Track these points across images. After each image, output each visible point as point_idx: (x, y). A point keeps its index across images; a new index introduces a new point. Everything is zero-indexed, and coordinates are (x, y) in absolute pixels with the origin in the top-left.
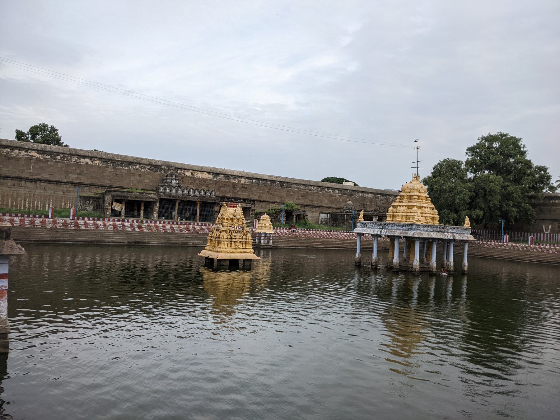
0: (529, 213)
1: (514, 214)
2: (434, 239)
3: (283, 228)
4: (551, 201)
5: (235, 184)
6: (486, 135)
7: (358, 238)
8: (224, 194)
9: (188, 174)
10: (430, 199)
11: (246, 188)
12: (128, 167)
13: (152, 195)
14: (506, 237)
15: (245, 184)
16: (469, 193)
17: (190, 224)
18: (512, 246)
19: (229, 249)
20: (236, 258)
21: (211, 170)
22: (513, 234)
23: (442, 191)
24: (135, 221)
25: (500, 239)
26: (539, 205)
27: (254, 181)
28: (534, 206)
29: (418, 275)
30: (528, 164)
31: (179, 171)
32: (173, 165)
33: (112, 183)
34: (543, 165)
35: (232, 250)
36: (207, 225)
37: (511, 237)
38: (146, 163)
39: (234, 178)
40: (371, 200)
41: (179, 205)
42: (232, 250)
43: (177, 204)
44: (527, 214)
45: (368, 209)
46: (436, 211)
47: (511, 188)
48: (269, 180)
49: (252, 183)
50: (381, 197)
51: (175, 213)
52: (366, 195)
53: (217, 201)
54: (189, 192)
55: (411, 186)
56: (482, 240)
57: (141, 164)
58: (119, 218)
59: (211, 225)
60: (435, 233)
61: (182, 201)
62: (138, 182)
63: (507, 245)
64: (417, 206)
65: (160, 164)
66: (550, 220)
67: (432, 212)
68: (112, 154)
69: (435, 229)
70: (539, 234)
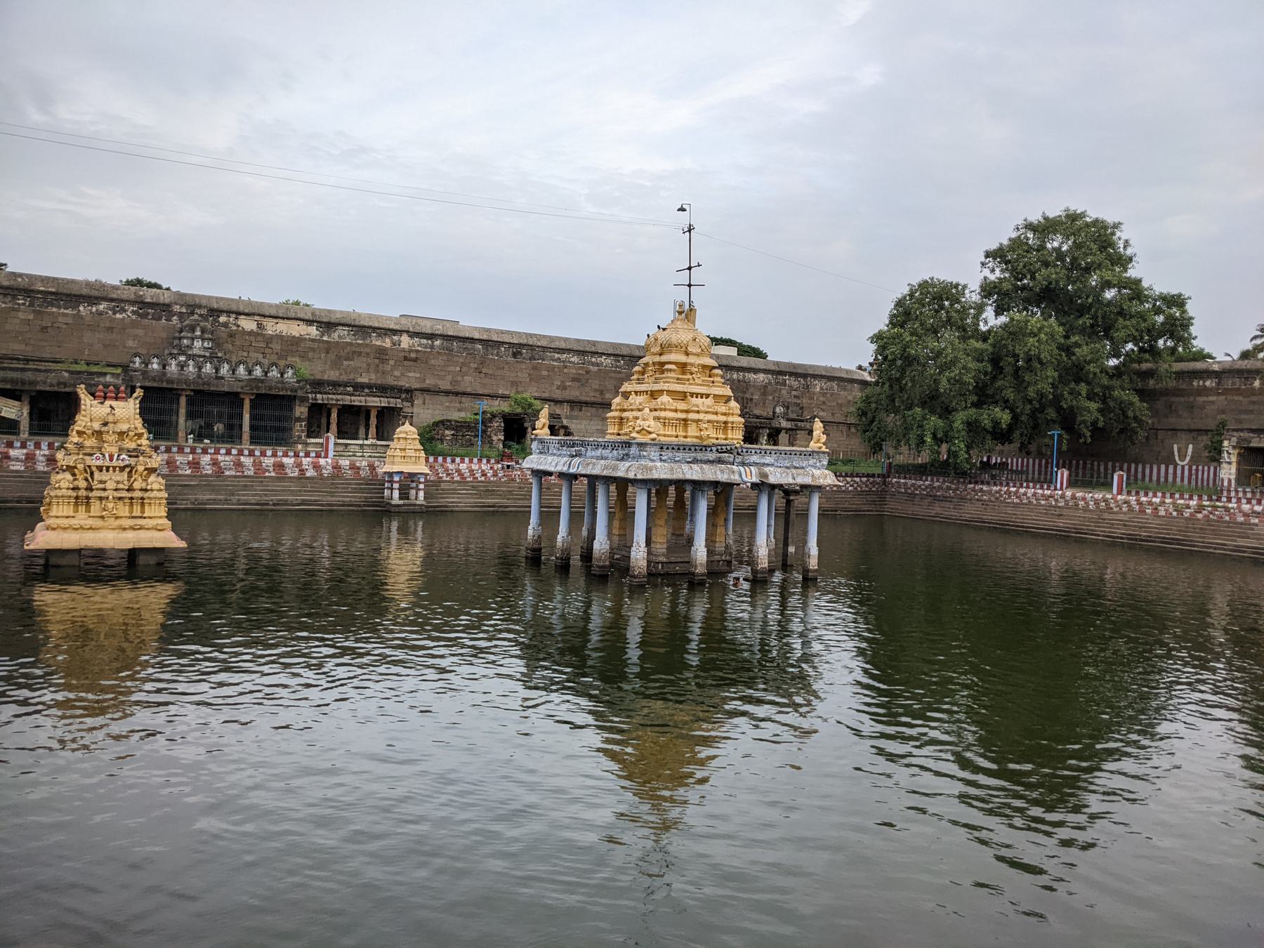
0: (1130, 414)
1: (1088, 418)
2: (698, 485)
3: (480, 461)
4: (1195, 383)
5: (382, 352)
6: (1035, 218)
7: (533, 481)
8: (352, 376)
9: (248, 324)
10: (718, 371)
11: (415, 360)
12: (75, 307)
13: (108, 379)
14: (1063, 475)
15: (410, 351)
16: (972, 365)
17: (205, 451)
18: (1073, 497)
19: (82, 518)
20: (100, 544)
21: (313, 314)
22: (1102, 468)
23: (909, 360)
24: (44, 446)
25: (1048, 481)
26: (1166, 392)
27: (438, 343)
28: (1143, 394)
29: (702, 583)
30: (1136, 290)
31: (222, 319)
32: (204, 302)
33: (29, 348)
34: (1174, 292)
35: (90, 522)
36: (257, 453)
37: (1077, 475)
38: (124, 297)
39: (379, 335)
40: (764, 389)
41: (190, 402)
42: (90, 522)
43: (183, 400)
44: (1127, 417)
45: (757, 412)
46: (733, 404)
47: (1083, 352)
48: (480, 340)
49: (432, 347)
50: (791, 381)
51: (299, 429)
52: (752, 376)
53: (300, 393)
54: (217, 370)
55: (662, 336)
56: (1008, 485)
57: (112, 300)
58: (12, 438)
59: (269, 453)
60: (695, 467)
61: (258, 395)
62: (105, 346)
63: (1063, 496)
64: (669, 392)
65: (167, 301)
66: (1190, 431)
67: (723, 409)
68: (30, 276)
69: (700, 456)
70: (1163, 467)
